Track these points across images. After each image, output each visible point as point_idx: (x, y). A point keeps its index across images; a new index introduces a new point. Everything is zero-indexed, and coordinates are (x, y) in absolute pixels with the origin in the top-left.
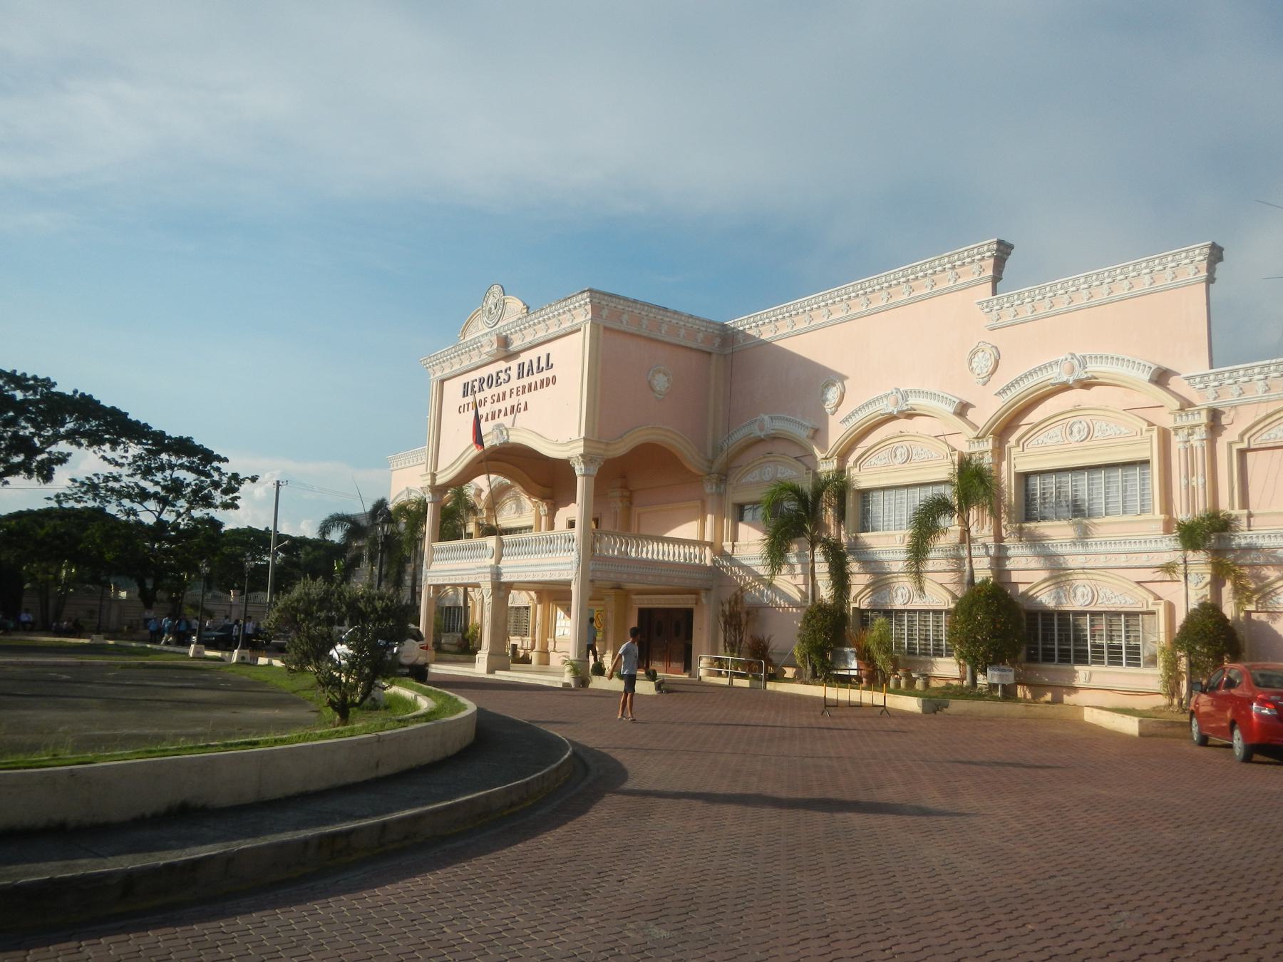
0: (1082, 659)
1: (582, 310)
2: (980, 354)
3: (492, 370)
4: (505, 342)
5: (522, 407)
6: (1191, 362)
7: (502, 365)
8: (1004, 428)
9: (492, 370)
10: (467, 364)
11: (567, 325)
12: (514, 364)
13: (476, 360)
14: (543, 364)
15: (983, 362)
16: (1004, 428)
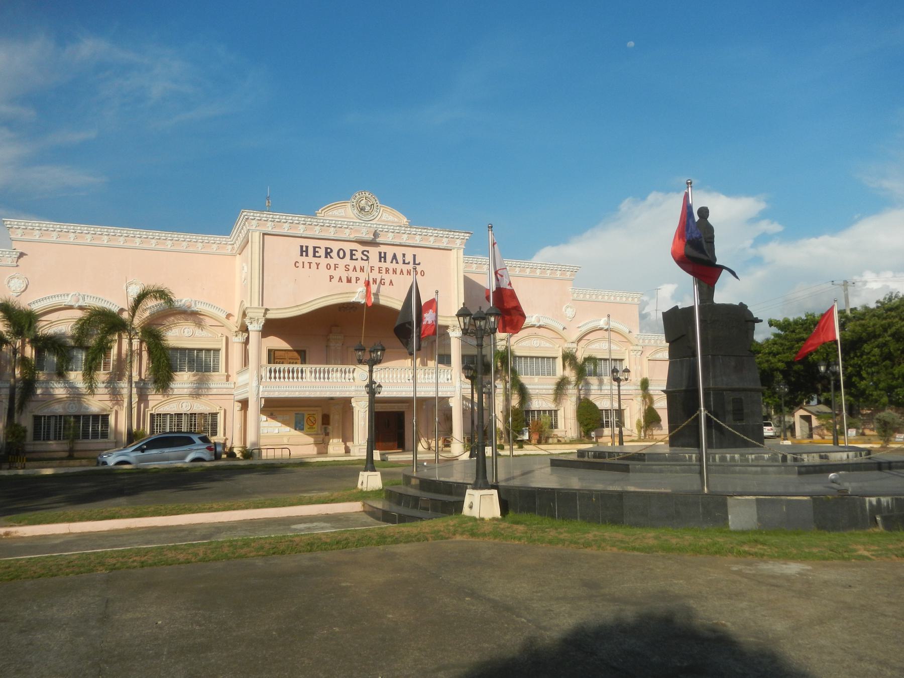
0: (602, 426)
1: (458, 241)
2: (569, 309)
3: (347, 247)
4: (376, 235)
5: (387, 282)
6: (636, 332)
7: (360, 248)
8: (580, 340)
9: (347, 247)
10: (316, 232)
11: (444, 243)
12: (373, 252)
13: (331, 233)
14: (409, 258)
15: (570, 312)
16: (580, 340)
